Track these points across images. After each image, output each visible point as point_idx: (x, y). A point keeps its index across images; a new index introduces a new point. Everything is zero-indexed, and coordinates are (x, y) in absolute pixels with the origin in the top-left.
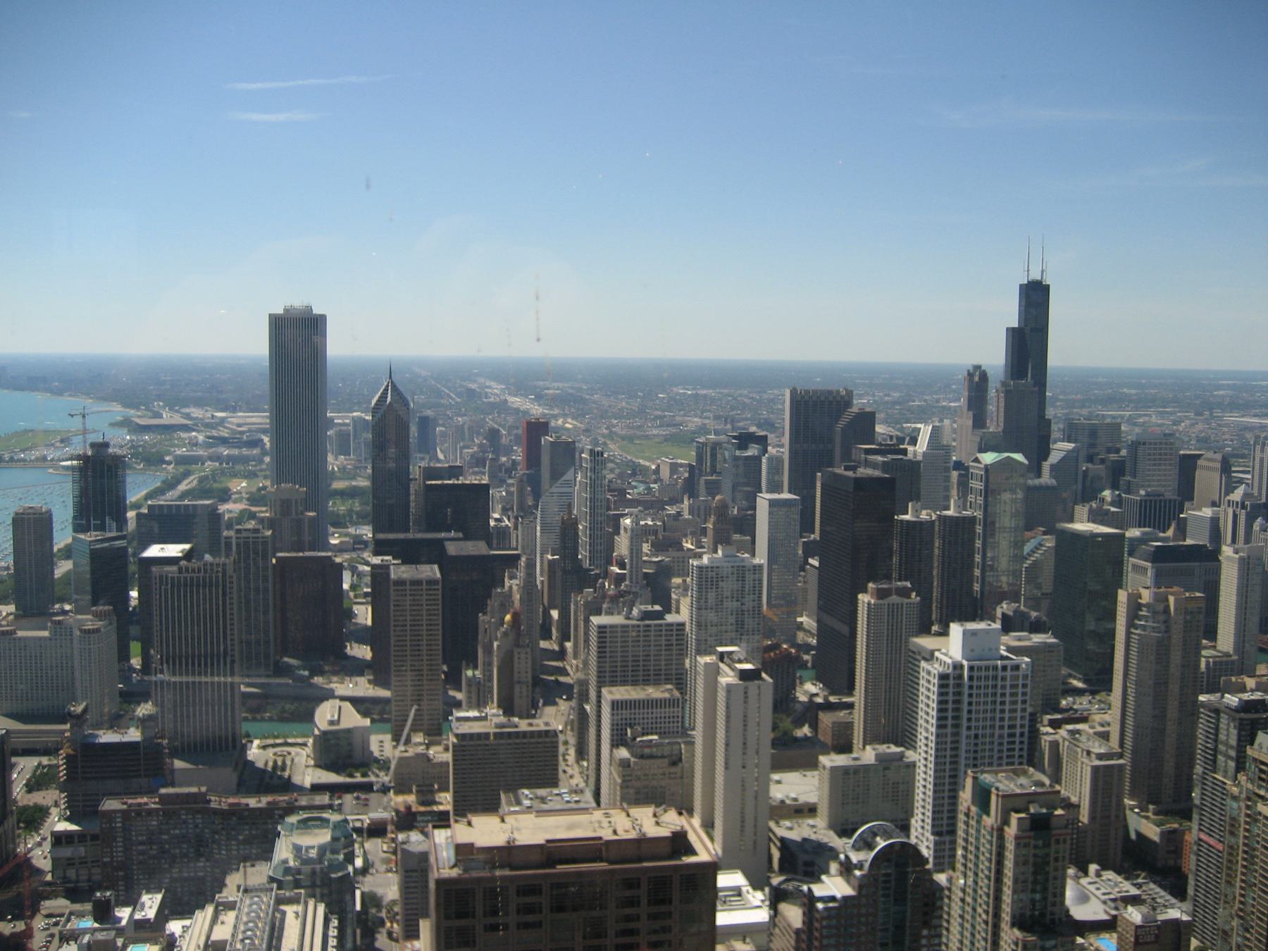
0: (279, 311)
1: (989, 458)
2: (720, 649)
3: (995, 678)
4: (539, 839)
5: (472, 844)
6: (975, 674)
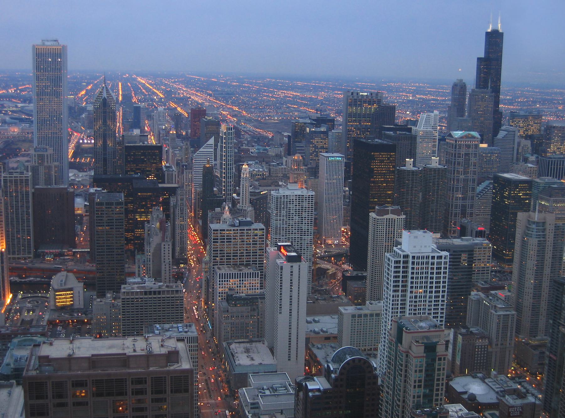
0: (39, 42)
1: (458, 134)
2: (279, 244)
3: (427, 263)
4: (88, 354)
5: (48, 357)
6: (416, 260)
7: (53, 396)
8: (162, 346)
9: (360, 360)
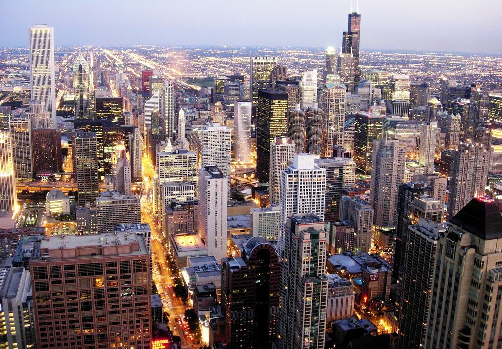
2: (207, 166)
3: (311, 176)
7: (51, 276)
8: (127, 239)
9: (266, 245)
